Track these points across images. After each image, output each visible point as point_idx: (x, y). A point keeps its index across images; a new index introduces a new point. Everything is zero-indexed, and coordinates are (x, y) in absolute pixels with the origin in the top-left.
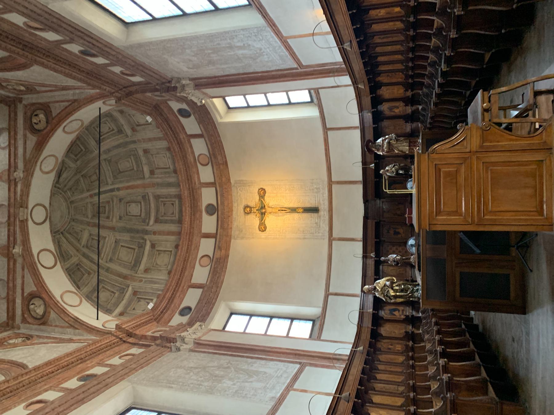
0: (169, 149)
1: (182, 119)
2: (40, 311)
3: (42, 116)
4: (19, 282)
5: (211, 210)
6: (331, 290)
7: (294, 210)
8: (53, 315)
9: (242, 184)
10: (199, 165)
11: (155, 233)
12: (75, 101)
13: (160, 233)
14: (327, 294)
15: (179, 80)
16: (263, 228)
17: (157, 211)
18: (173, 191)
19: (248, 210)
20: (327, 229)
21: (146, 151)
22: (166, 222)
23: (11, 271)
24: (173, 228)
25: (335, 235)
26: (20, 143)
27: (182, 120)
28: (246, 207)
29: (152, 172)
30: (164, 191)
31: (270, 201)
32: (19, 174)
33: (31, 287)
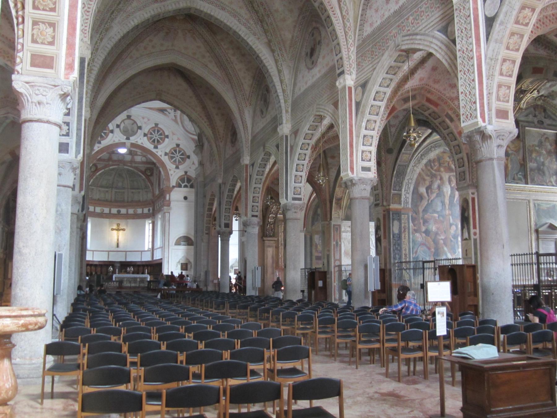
3: (149, 174)
4: (101, 162)
5: (119, 212)
6: (94, 252)
7: (118, 240)
9: (127, 225)
10: (133, 210)
11: (111, 192)
12: (153, 184)
14: (93, 251)
15: (154, 218)
16: (113, 229)
17: (119, 192)
19: (118, 225)
20: (111, 250)
21: (139, 192)
25: (110, 252)
28: (119, 224)
29: (133, 192)
31: (121, 232)
32: (134, 165)
33: (99, 166)
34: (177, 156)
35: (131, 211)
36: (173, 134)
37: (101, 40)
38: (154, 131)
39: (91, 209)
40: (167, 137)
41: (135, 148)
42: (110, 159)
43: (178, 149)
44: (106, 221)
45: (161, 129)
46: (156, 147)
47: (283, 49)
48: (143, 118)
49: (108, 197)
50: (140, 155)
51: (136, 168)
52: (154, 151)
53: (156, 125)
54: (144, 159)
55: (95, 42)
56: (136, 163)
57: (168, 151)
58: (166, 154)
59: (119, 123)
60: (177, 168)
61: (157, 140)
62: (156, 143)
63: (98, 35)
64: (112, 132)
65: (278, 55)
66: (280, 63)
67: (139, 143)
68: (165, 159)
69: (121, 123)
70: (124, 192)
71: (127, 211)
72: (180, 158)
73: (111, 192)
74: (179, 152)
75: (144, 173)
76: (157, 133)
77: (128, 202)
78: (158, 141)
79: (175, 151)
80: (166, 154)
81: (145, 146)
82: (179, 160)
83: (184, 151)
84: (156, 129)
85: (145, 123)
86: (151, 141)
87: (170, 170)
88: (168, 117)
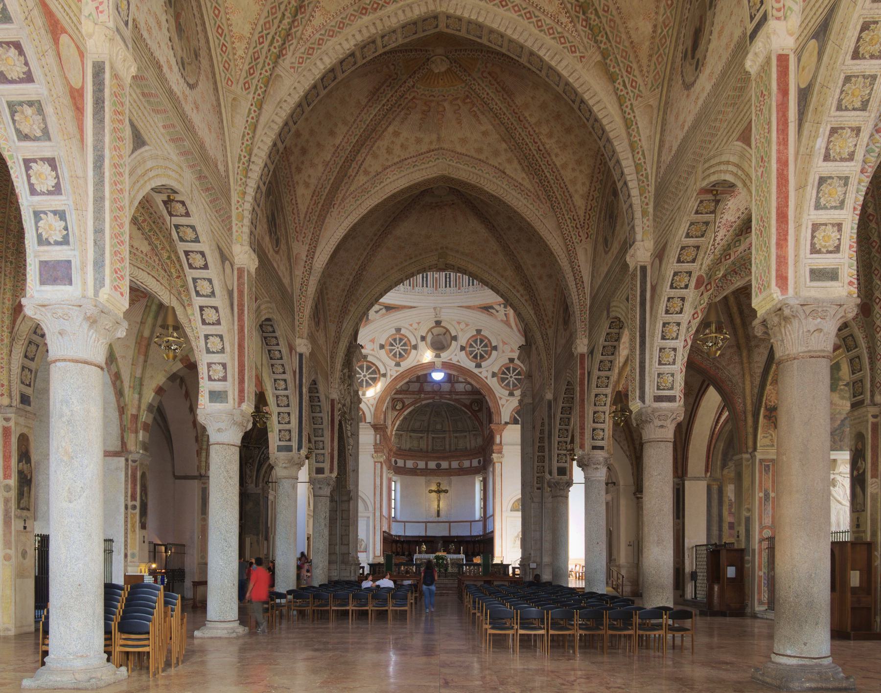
0: (466, 448)
1: (477, 460)
2: (398, 408)
4: (407, 396)
8: (396, 413)
9: (450, 484)
11: (427, 437)
12: (482, 423)
13: (427, 440)
17: (438, 438)
18: (447, 447)
22: (433, 443)
23: (413, 393)
24: (430, 448)
26: (467, 397)
27: (477, 460)
29: (456, 437)
30: (447, 443)
32: (454, 397)
34: (511, 377)
35: (455, 464)
36: (504, 343)
37: (260, 105)
38: (475, 342)
39: (400, 463)
40: (495, 348)
41: (454, 372)
42: (421, 391)
43: (511, 365)
44: (421, 480)
45: (486, 338)
46: (479, 366)
47: (635, 66)
48: (459, 323)
49: (423, 445)
50: (462, 382)
51: (456, 400)
52: (476, 371)
53: (479, 331)
54: (468, 388)
55: (247, 111)
56: (457, 393)
57: (496, 370)
58: (494, 375)
59: (424, 335)
60: (511, 394)
61: (481, 355)
62: (479, 359)
63: (251, 96)
64: (415, 347)
65: (625, 86)
66: (628, 103)
67: (454, 361)
68: (493, 383)
69: (427, 333)
70: (444, 438)
71: (450, 465)
72: (516, 379)
73: (427, 437)
74: (514, 370)
75: (469, 407)
76: (480, 344)
77: (450, 452)
78: (482, 357)
79: (508, 369)
80: (494, 375)
81: (462, 365)
82: (513, 383)
83: (520, 367)
84: (479, 338)
85: (462, 330)
86: (471, 357)
87: (501, 398)
88: (496, 318)
